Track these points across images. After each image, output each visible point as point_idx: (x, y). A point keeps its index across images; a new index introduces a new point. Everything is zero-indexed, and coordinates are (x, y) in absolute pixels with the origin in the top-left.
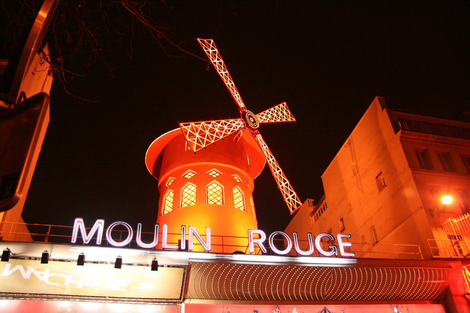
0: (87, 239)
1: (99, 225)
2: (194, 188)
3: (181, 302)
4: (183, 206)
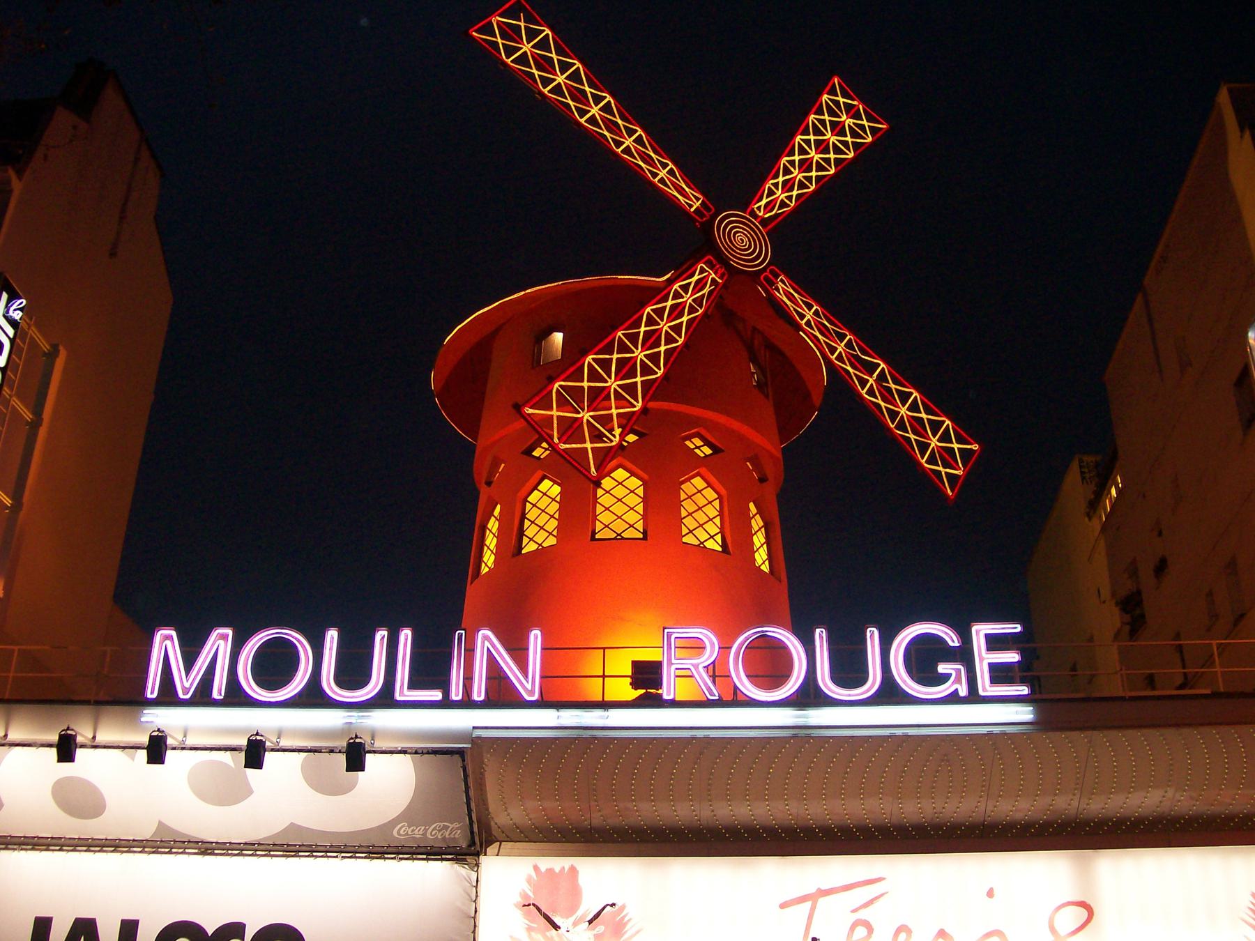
0: (187, 685)
1: (219, 642)
2: (556, 490)
3: (476, 852)
4: (523, 552)
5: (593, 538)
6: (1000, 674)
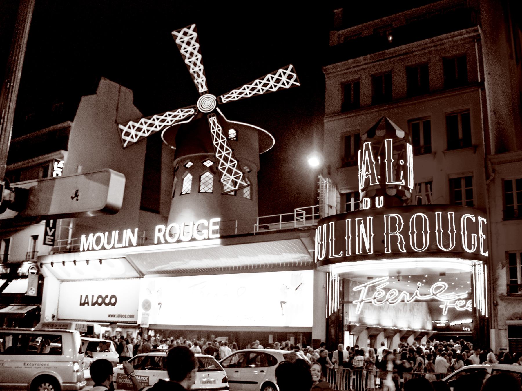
5: (181, 194)
6: (214, 232)
